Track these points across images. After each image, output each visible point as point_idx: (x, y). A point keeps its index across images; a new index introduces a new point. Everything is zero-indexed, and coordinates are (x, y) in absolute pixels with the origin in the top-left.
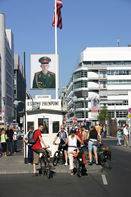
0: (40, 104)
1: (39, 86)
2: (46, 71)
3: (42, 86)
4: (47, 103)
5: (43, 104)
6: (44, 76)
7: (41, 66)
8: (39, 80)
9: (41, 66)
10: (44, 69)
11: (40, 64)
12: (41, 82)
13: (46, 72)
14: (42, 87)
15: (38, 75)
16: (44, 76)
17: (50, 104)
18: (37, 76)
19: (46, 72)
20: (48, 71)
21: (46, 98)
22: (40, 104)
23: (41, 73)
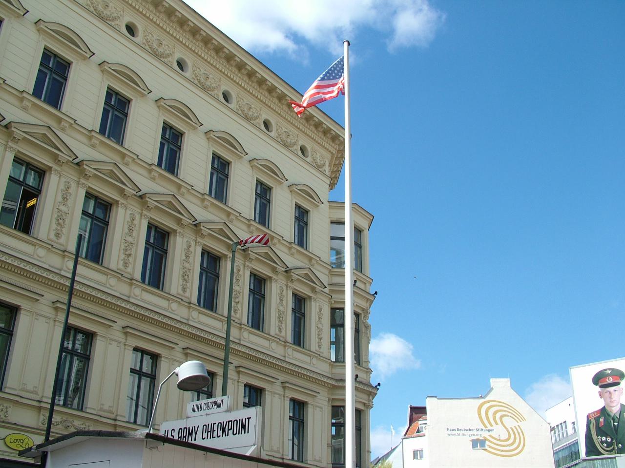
0: (196, 433)
1: (604, 450)
2: (614, 405)
3: (611, 448)
4: (216, 426)
5: (205, 435)
6: (613, 419)
7: (600, 395)
8: (601, 432)
9: (601, 395)
10: (608, 400)
11: (597, 389)
12: (606, 437)
13: (615, 410)
14: (610, 451)
15: (597, 420)
16: (613, 419)
17: (224, 431)
18: (593, 422)
19: (615, 410)
20: (621, 404)
21: (215, 410)
22: (196, 433)
23: (603, 411)
